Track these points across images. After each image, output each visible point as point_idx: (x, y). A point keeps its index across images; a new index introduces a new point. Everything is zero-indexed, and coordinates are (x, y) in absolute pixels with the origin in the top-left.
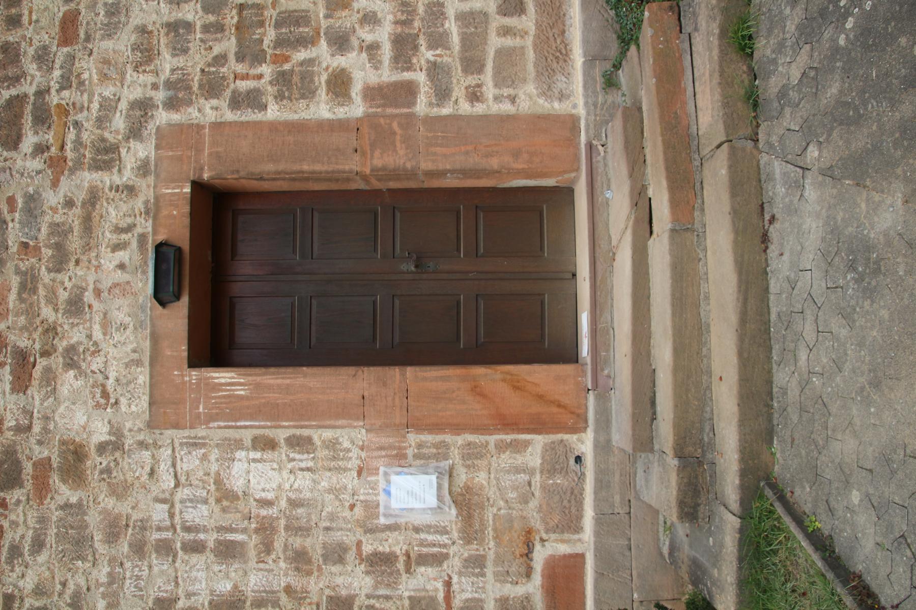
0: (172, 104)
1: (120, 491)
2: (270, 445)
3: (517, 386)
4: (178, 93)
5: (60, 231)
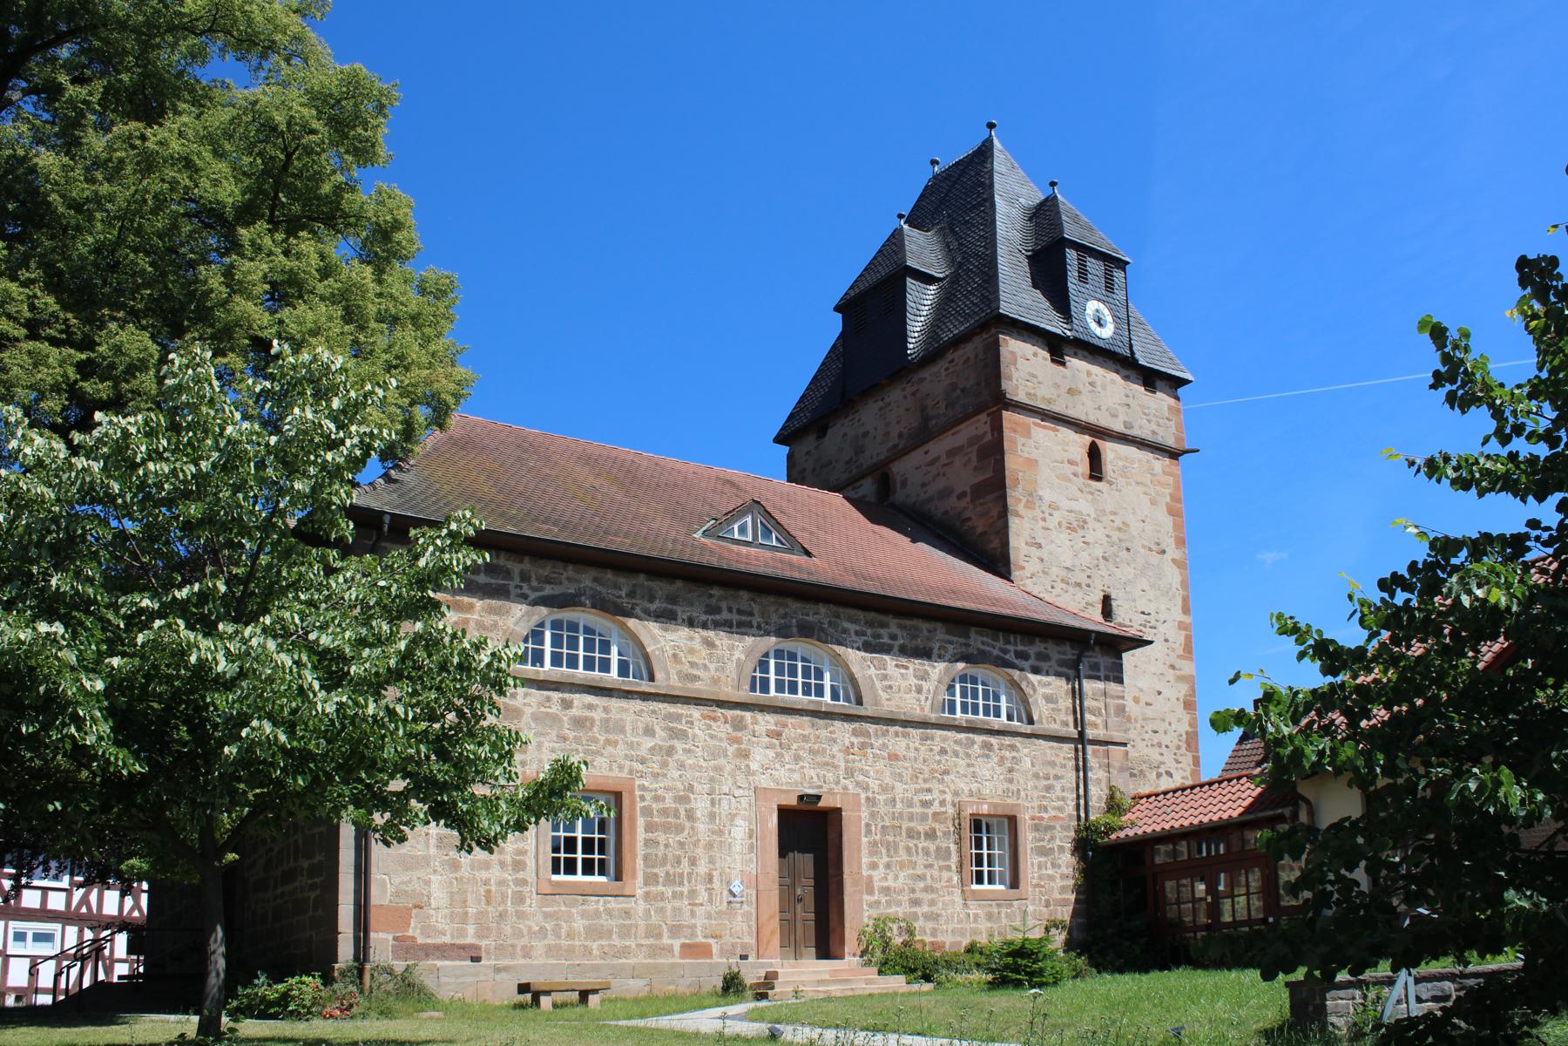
3: (772, 933)
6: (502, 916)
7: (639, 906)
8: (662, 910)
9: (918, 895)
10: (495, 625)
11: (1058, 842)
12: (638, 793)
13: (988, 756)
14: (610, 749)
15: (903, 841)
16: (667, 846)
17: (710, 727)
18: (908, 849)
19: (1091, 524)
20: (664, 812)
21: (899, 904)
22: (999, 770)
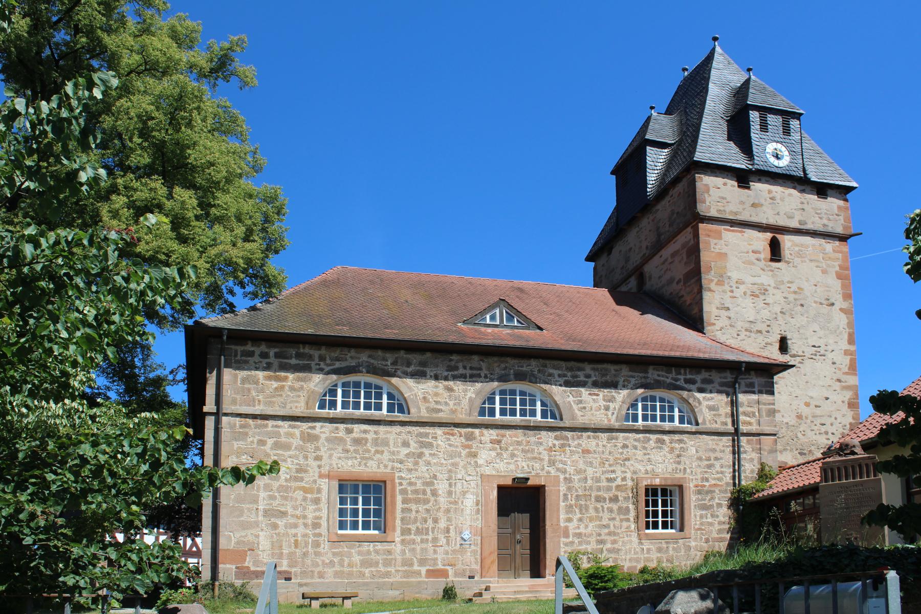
0: (565, 478)
1: (465, 467)
2: (477, 505)
4: (568, 480)
5: (533, 450)
6: (305, 554)
7: (398, 548)
8: (414, 550)
9: (603, 537)
10: (302, 388)
11: (717, 501)
12: (397, 481)
13: (660, 448)
14: (378, 456)
15: (592, 504)
16: (417, 512)
17: (449, 439)
18: (596, 509)
19: (771, 290)
20: (416, 492)
21: (588, 543)
22: (669, 456)
